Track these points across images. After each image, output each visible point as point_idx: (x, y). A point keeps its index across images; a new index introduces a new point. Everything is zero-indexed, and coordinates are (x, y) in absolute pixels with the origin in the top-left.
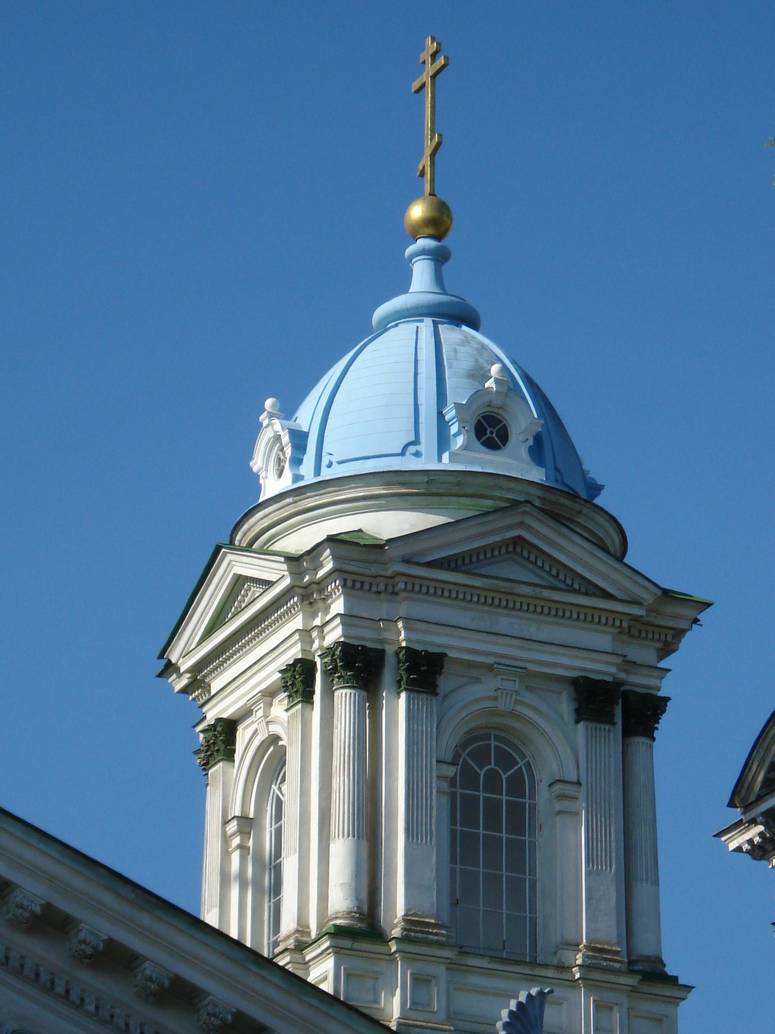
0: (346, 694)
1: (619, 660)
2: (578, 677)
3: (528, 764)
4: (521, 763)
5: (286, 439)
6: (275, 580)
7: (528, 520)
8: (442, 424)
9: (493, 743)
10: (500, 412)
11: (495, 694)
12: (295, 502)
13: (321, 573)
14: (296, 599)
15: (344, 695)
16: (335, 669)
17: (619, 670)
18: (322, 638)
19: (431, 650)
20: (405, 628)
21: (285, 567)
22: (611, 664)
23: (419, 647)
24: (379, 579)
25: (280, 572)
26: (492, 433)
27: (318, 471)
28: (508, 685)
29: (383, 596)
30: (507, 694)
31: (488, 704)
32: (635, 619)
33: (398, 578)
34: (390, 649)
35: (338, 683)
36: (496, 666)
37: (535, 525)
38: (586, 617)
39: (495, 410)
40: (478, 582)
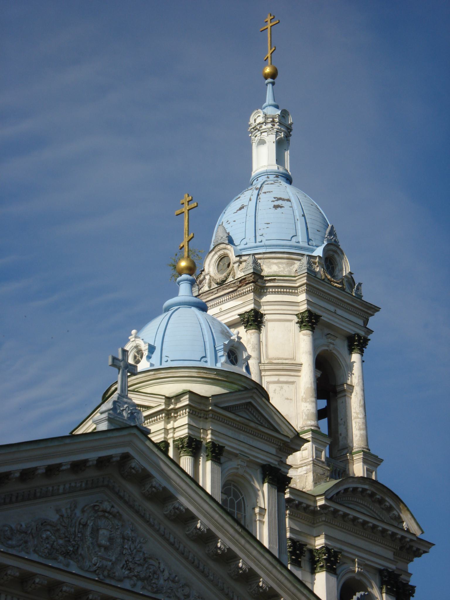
0: (188, 458)
1: (278, 459)
2: (266, 464)
3: (243, 498)
4: (241, 497)
5: (144, 348)
6: (154, 406)
7: (255, 396)
8: (216, 352)
9: (232, 488)
10: (236, 350)
11: (237, 466)
12: (155, 374)
13: (179, 405)
14: (164, 415)
15: (187, 459)
16: (182, 448)
17: (279, 464)
18: (174, 433)
19: (221, 444)
20: (212, 434)
21: (164, 401)
22: (276, 460)
23: (216, 443)
24: (202, 411)
25: (157, 403)
26: (232, 358)
27: (161, 364)
28: (242, 463)
29: (201, 419)
30: (242, 467)
31: (235, 471)
32: (285, 443)
33: (210, 412)
34: (204, 443)
35: (183, 453)
36: (239, 455)
37: (256, 398)
38: (269, 439)
39: (234, 349)
40: (238, 419)
